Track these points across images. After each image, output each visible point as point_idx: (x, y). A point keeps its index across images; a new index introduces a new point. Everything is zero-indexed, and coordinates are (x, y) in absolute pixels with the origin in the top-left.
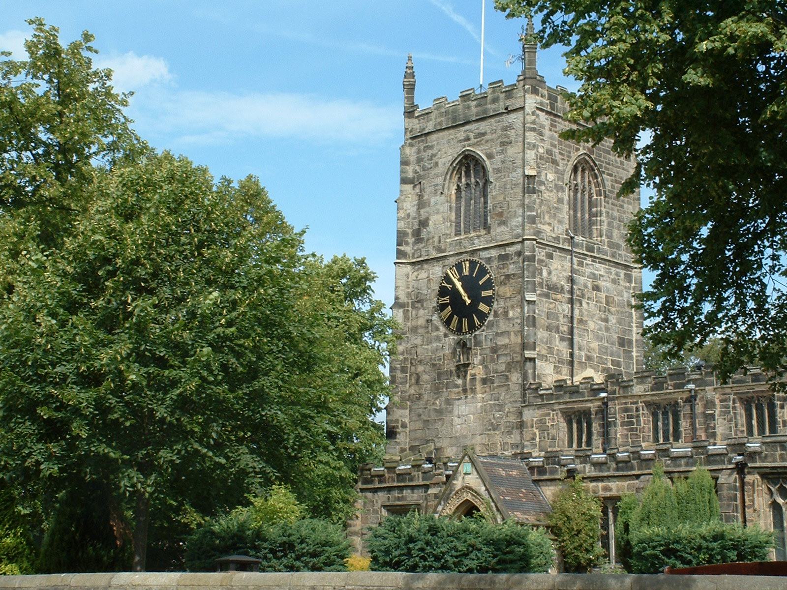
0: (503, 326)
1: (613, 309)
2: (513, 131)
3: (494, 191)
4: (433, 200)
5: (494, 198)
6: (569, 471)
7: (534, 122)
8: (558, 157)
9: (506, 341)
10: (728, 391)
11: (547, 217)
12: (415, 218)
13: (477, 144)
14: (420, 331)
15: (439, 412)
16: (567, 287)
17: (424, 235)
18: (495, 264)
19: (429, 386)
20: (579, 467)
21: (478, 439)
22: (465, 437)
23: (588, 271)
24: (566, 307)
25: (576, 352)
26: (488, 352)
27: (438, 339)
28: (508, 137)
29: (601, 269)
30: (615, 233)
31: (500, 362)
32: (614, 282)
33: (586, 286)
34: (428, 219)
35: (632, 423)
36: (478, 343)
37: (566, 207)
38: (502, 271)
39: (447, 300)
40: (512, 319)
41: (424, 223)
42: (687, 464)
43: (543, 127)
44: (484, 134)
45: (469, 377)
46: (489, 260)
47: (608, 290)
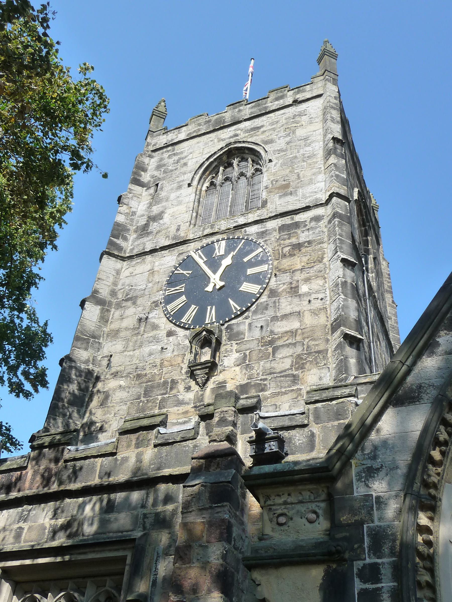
0: (286, 305)
4: (173, 196)
9: (294, 324)
12: (143, 215)
14: (122, 334)
17: (154, 227)
19: (125, 407)
26: (254, 345)
27: (156, 340)
31: (279, 355)
36: (235, 336)
38: (287, 242)
40: (309, 294)
45: (211, 385)
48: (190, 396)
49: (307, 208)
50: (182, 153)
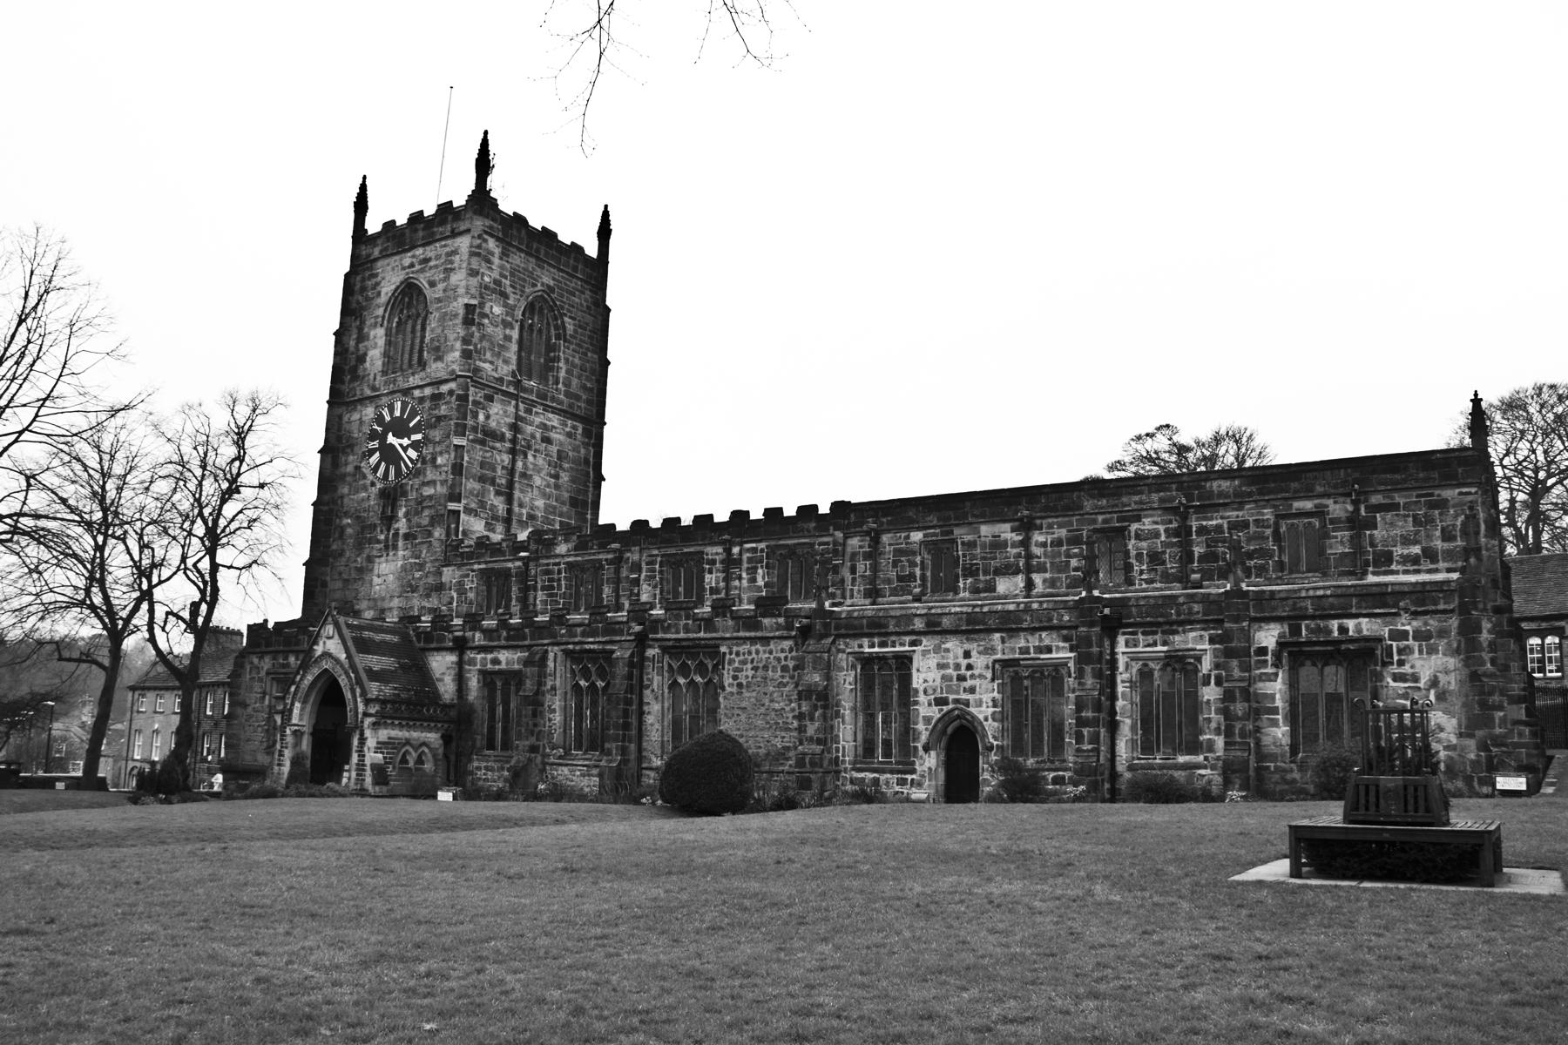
0: (430, 475)
1: (566, 466)
2: (457, 258)
3: (433, 323)
4: (372, 333)
5: (432, 330)
6: (456, 639)
7: (479, 247)
8: (509, 290)
10: (656, 552)
11: (488, 356)
13: (422, 271)
15: (360, 570)
16: (508, 435)
18: (427, 404)
20: (469, 634)
21: (396, 602)
22: (383, 599)
23: (538, 420)
24: (506, 458)
25: (516, 509)
27: (365, 488)
28: (452, 262)
29: (554, 420)
30: (575, 381)
32: (569, 435)
33: (533, 436)
34: (365, 354)
35: (552, 588)
36: (404, 494)
37: (514, 347)
39: (376, 444)
41: (362, 359)
42: (583, 634)
43: (492, 254)
44: (426, 260)
46: (422, 400)
47: (561, 444)
48: (382, 537)
49: (446, 381)
50: (376, 275)
